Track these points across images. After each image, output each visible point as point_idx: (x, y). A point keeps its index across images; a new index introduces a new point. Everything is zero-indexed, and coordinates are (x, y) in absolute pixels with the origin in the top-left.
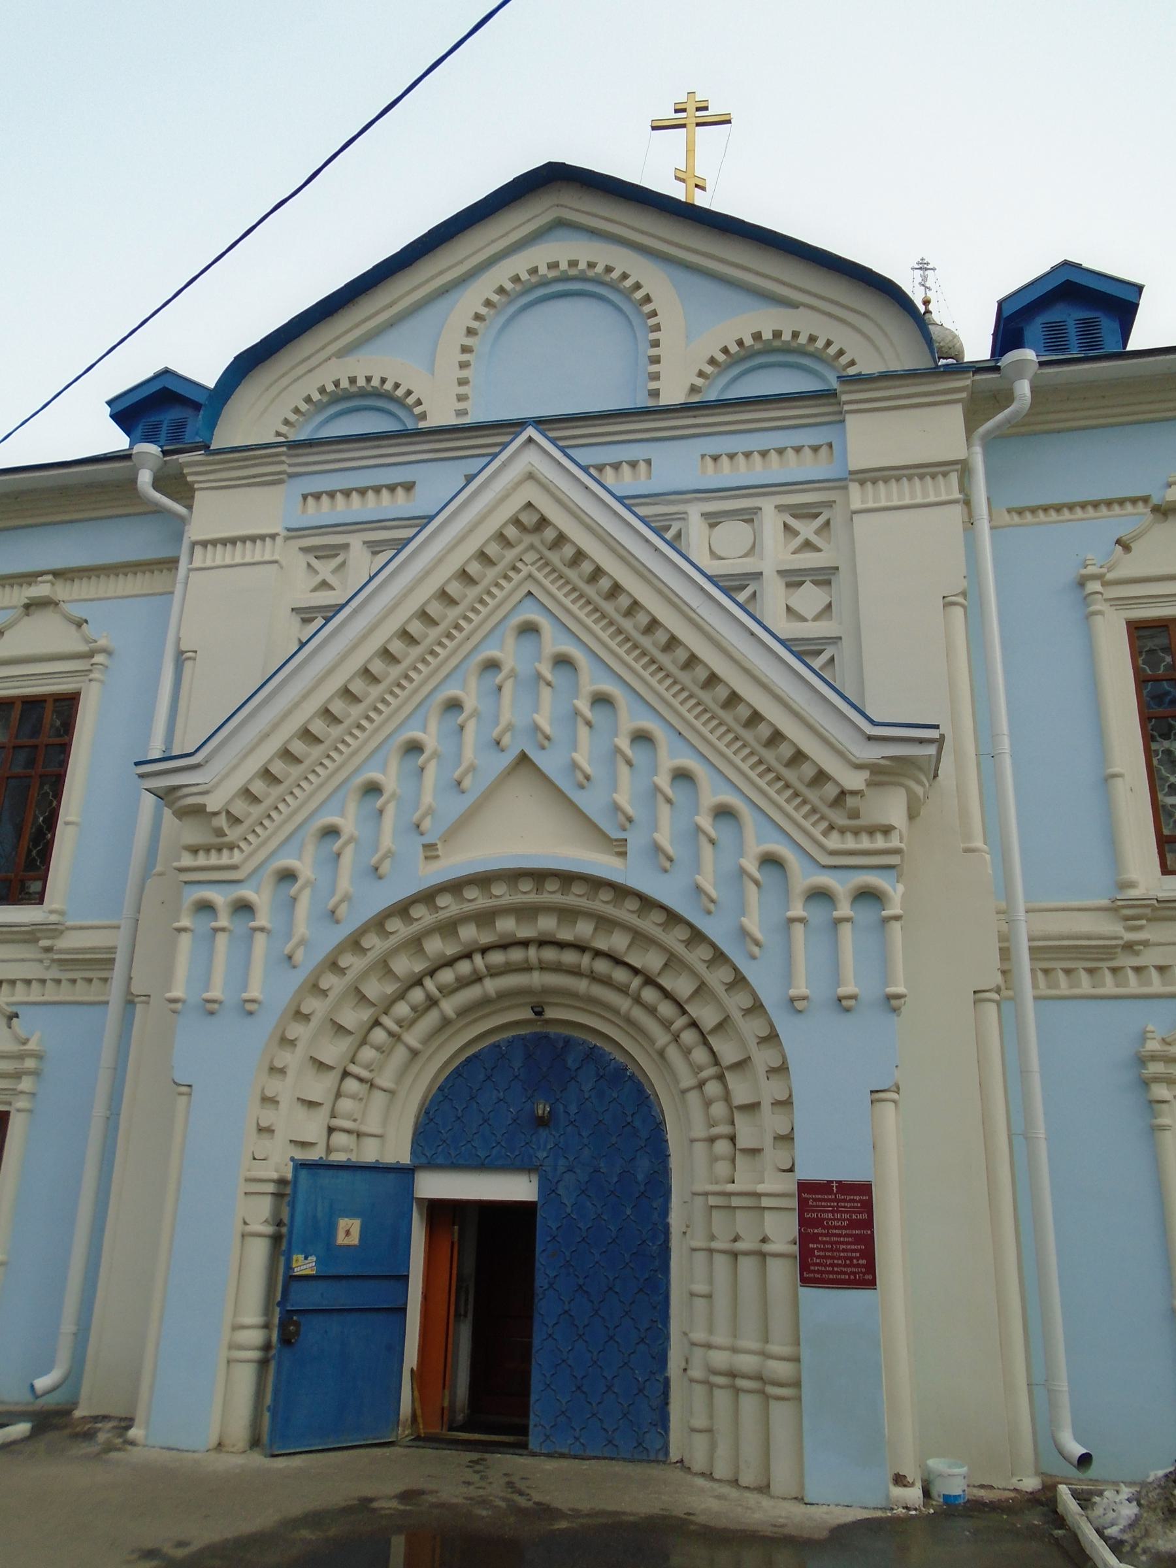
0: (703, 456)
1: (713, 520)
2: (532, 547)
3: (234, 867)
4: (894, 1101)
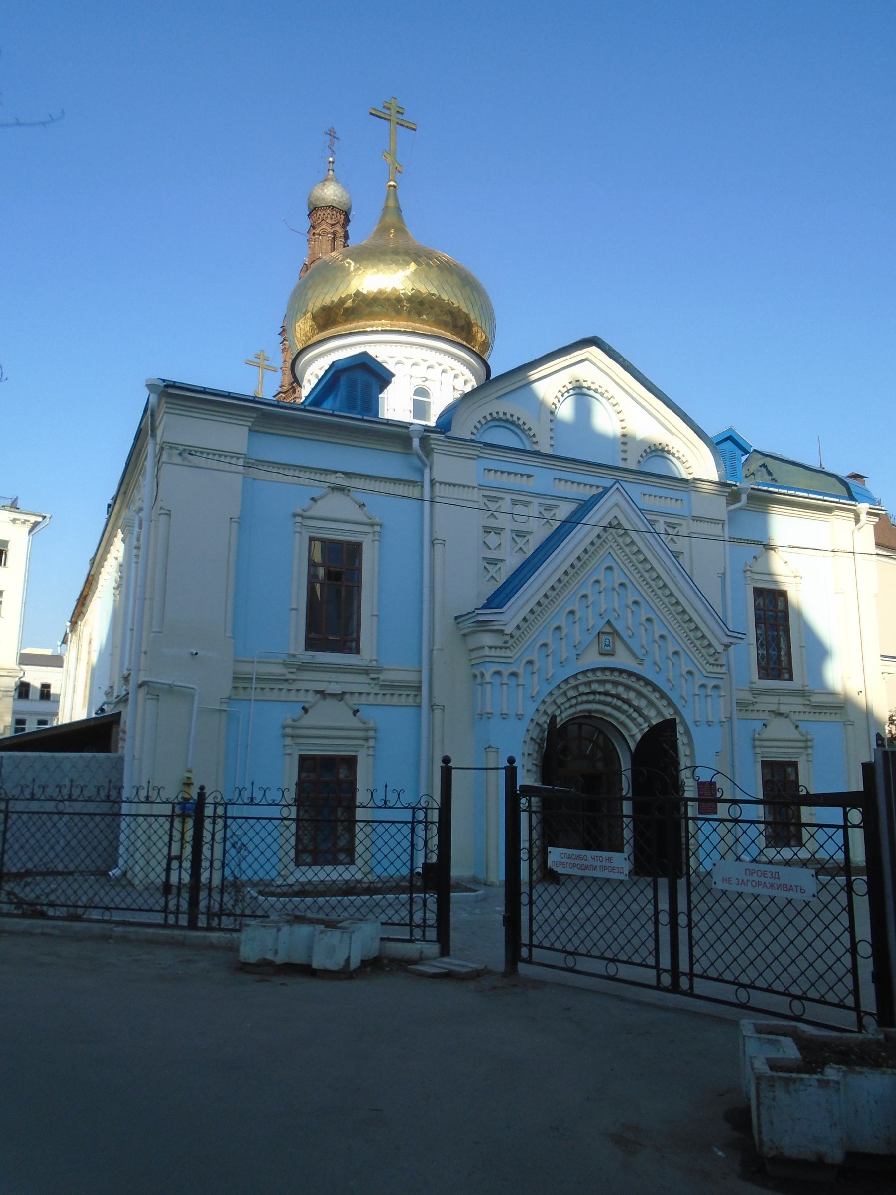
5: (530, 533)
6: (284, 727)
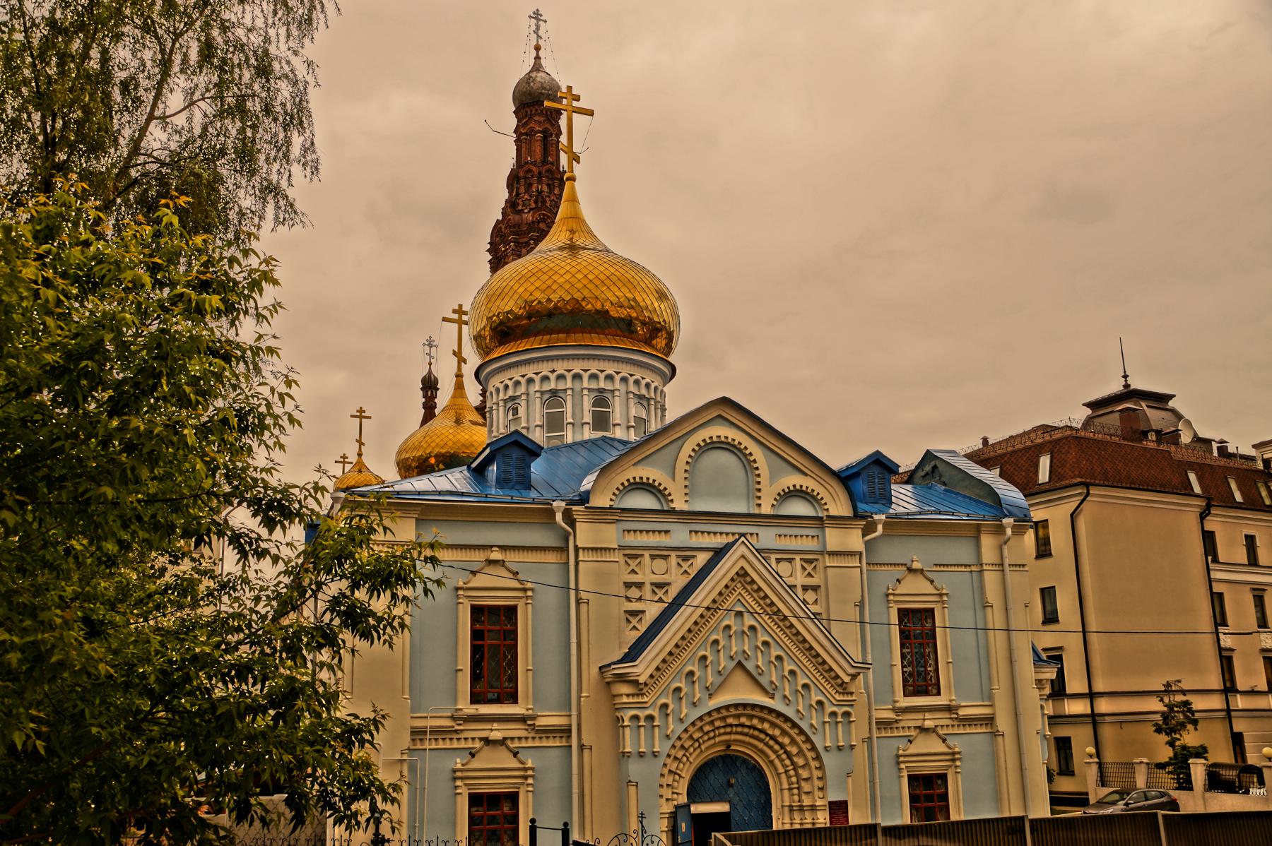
5: (669, 584)
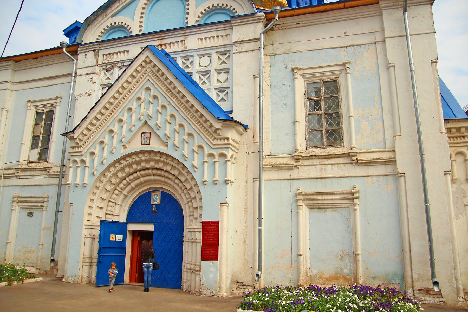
0: (198, 39)
1: (201, 56)
2: (149, 67)
3: (81, 152)
4: (227, 206)
6: (14, 197)
